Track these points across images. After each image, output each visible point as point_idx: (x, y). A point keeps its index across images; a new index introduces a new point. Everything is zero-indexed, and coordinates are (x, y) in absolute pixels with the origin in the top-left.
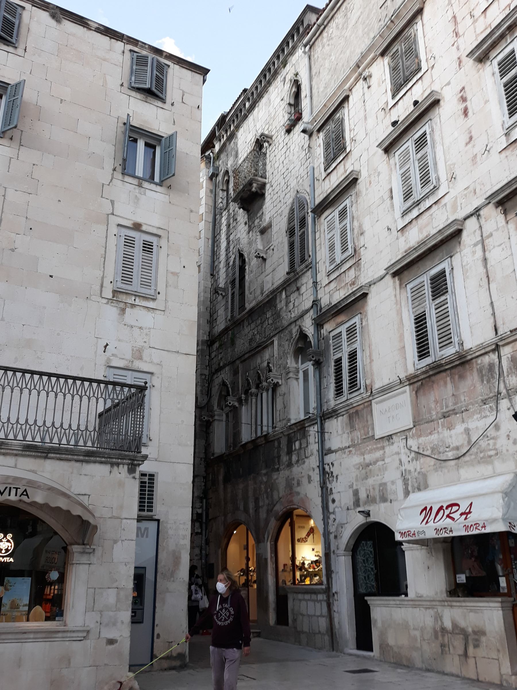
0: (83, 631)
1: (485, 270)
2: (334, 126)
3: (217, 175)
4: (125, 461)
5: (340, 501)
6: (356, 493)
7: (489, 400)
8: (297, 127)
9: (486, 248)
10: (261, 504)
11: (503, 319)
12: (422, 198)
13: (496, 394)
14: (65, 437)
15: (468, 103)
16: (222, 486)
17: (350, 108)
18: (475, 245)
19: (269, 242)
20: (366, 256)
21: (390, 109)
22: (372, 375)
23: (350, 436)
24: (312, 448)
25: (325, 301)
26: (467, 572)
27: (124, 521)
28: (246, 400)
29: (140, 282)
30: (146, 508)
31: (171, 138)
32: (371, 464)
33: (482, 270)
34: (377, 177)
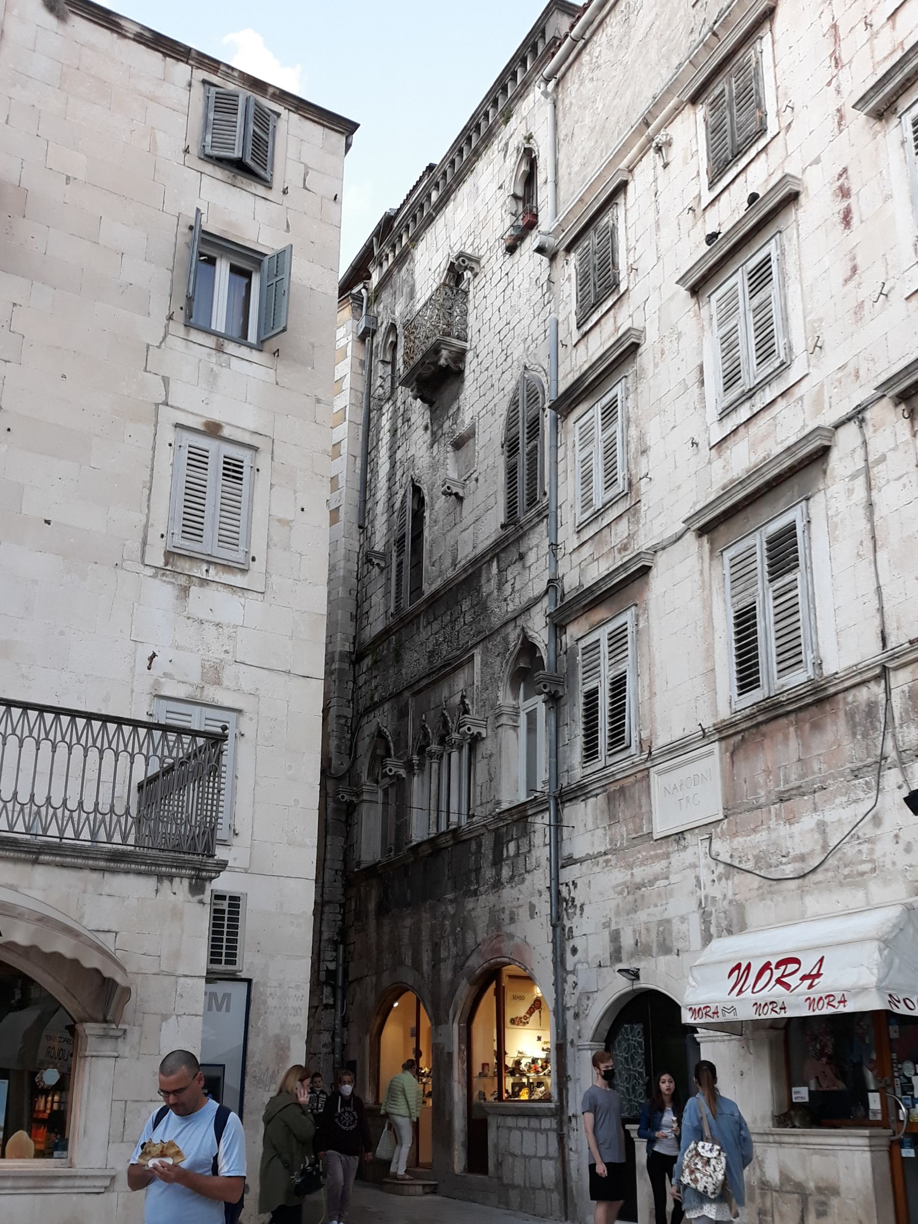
0: (105, 1177)
1: (869, 526)
2: (597, 241)
3: (374, 332)
4: (184, 871)
5: (586, 951)
6: (615, 937)
7: (865, 769)
8: (528, 241)
9: (873, 483)
10: (443, 954)
11: (898, 620)
12: (758, 384)
13: (878, 759)
14: (70, 824)
15: (852, 201)
16: (373, 923)
17: (628, 206)
18: (853, 477)
19: (469, 465)
20: (649, 494)
21: (705, 209)
22: (652, 721)
23: (609, 833)
24: (538, 854)
25: (571, 581)
26: (813, 1083)
27: (182, 980)
28: (421, 765)
29: (217, 537)
30: (223, 958)
31: (282, 258)
32: (644, 885)
33: (863, 525)
34: (675, 343)
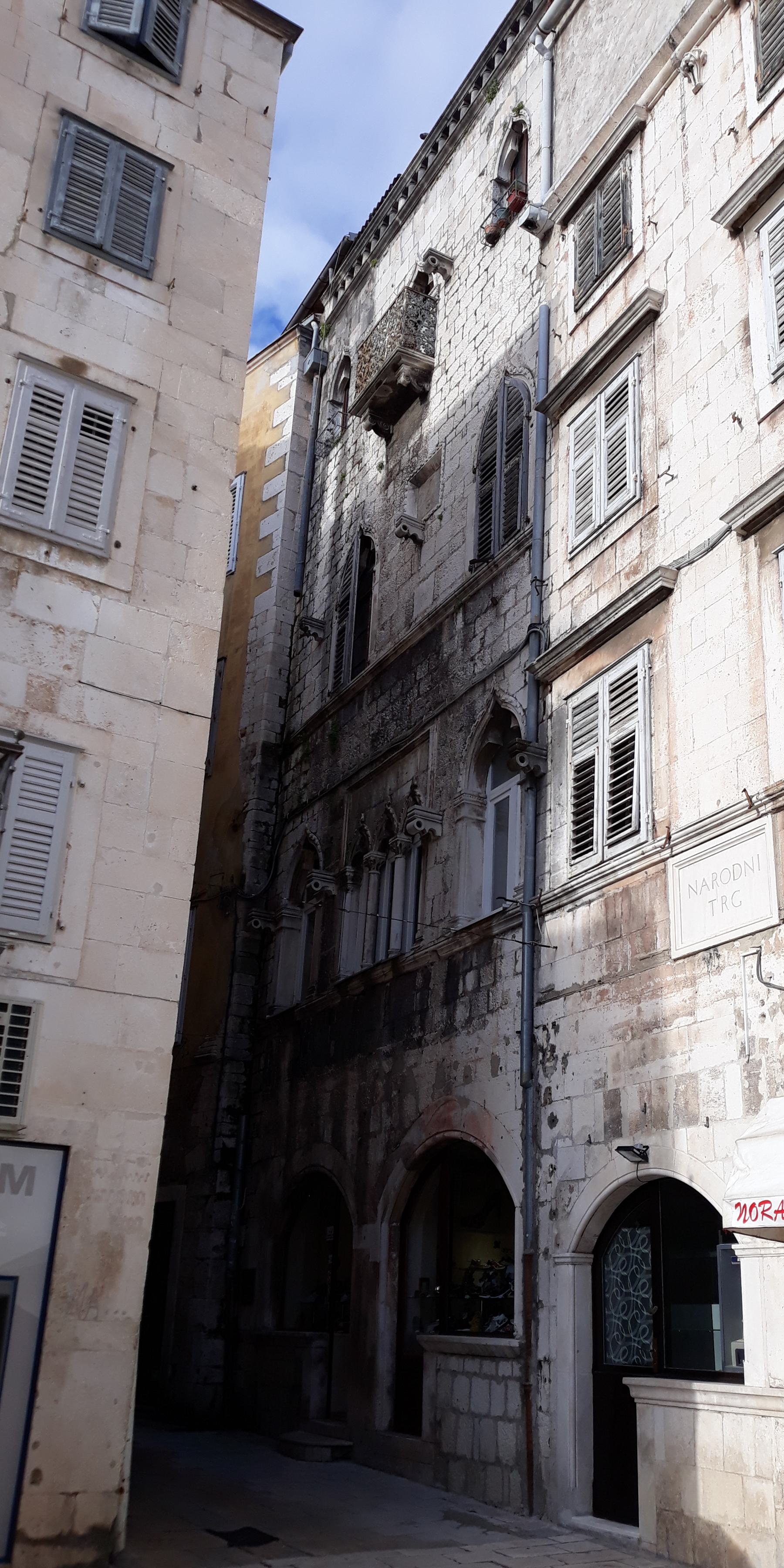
5: (570, 1121)
6: (613, 1100)
17: (645, 152)
19: (432, 501)
21: (751, 128)
23: (606, 953)
24: (506, 988)
28: (357, 880)
